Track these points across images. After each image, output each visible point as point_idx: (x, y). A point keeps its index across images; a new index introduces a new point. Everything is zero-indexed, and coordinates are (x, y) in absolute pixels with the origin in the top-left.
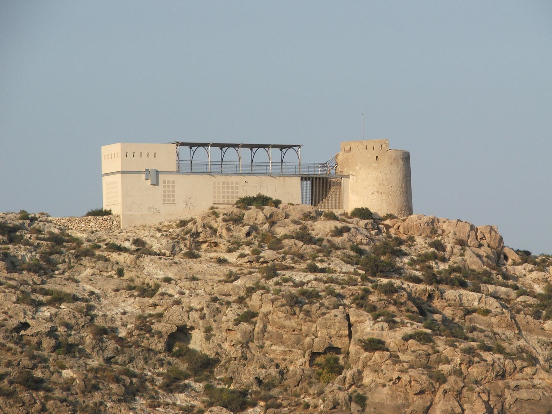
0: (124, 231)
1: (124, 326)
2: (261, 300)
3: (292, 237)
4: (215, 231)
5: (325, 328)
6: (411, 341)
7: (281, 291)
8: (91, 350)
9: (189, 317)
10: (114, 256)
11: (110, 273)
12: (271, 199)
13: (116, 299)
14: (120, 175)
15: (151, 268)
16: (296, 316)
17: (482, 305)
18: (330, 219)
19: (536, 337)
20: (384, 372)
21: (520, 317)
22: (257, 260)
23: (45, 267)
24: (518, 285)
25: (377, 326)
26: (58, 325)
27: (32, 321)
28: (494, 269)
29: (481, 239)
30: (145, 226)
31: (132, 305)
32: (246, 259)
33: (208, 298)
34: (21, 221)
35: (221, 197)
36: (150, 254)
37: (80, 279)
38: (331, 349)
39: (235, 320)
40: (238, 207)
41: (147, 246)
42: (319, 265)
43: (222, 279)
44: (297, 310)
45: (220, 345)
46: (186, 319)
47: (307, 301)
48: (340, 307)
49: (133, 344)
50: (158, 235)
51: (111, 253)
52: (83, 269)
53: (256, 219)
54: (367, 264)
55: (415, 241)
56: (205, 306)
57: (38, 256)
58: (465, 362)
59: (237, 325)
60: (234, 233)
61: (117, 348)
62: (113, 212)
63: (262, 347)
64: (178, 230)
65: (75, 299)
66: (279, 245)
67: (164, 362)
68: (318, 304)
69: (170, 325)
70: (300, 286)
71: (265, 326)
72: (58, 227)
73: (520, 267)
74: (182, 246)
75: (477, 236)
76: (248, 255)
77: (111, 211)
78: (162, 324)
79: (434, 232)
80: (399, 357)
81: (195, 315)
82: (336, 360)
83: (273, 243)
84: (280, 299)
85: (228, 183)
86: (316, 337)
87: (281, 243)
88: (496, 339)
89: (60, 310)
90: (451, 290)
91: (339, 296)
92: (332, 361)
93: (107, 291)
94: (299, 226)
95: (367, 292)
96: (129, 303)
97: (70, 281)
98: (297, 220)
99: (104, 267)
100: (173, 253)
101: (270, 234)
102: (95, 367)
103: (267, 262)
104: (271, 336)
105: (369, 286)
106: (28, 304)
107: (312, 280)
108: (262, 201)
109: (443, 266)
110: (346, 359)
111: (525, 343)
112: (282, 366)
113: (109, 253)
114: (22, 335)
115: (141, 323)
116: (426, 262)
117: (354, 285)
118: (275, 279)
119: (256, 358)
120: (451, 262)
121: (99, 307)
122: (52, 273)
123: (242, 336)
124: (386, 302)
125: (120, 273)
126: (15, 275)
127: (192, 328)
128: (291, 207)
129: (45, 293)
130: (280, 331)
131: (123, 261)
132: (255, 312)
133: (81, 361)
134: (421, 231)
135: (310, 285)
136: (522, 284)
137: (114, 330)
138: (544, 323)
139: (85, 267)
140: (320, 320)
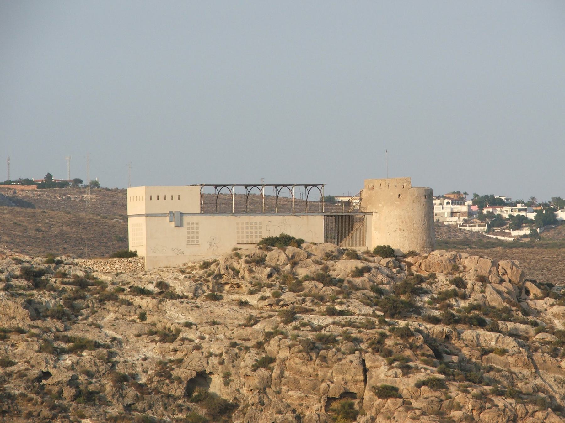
0: (148, 273)
1: (144, 372)
2: (279, 346)
3: (313, 279)
4: (237, 273)
5: (341, 373)
6: (423, 388)
7: (298, 336)
8: (111, 397)
9: (208, 363)
10: (137, 300)
11: (132, 318)
12: (294, 238)
13: (137, 344)
14: (144, 218)
15: (173, 313)
16: (312, 362)
17: (500, 345)
18: (351, 258)
19: (552, 375)
20: (396, 419)
21: (538, 356)
22: (277, 304)
23: (69, 313)
24: (538, 321)
25: (391, 372)
26: (79, 373)
27: (54, 370)
28: (514, 306)
29: (503, 274)
30: (169, 267)
31: (153, 351)
32: (266, 302)
33: (228, 343)
34: (46, 265)
35: (245, 237)
36: (172, 298)
37: (103, 325)
38: (347, 394)
39: (253, 366)
40: (260, 248)
41: (170, 289)
42: (338, 307)
43: (242, 322)
44: (314, 356)
45: (238, 390)
46: (205, 365)
47: (324, 347)
48: (357, 352)
49: (153, 390)
50: (182, 277)
51: (134, 297)
52: (107, 313)
53: (278, 260)
54: (386, 305)
55: (436, 278)
56: (224, 351)
57: (62, 302)
58: (476, 408)
59: (254, 370)
60: (256, 275)
61: (137, 395)
62: (138, 253)
63: (279, 393)
64: (201, 272)
65: (97, 345)
66: (300, 287)
67: (183, 408)
68: (334, 350)
69: (190, 371)
70: (318, 330)
71: (282, 372)
72: (83, 269)
73: (541, 302)
74: (205, 288)
75: (498, 272)
76: (269, 297)
77: (136, 252)
78: (181, 370)
79: (455, 268)
80: (411, 404)
81: (214, 360)
82: (351, 406)
83: (293, 284)
84: (298, 345)
85: (251, 223)
86: (332, 382)
87: (301, 285)
88: (513, 378)
89: (82, 357)
90: (469, 331)
91: (357, 341)
92: (347, 407)
93: (129, 336)
94: (321, 266)
95: (383, 336)
96: (150, 348)
97: (93, 327)
98: (319, 260)
99: (127, 311)
100: (196, 296)
101: (291, 276)
102: (114, 416)
103: (287, 305)
104: (288, 382)
105: (386, 330)
106: (50, 353)
107: (330, 324)
108: (285, 241)
109: (463, 304)
110: (361, 405)
111: (541, 382)
112: (299, 411)
113: (132, 297)
114: (44, 385)
115: (161, 370)
116: (446, 300)
117: (372, 329)
118: (294, 324)
119: (272, 404)
120: (471, 300)
121: (120, 354)
122: (75, 319)
123: (260, 382)
124: (402, 346)
125: (143, 317)
126: (39, 323)
127: (211, 373)
128: (314, 247)
129: (68, 340)
130: (297, 377)
131: (145, 305)
132: (273, 357)
133: (101, 410)
134: (442, 268)
135: (327, 329)
136: (542, 320)
137: (134, 377)
138: (561, 361)
139: (108, 311)
140: (336, 366)
